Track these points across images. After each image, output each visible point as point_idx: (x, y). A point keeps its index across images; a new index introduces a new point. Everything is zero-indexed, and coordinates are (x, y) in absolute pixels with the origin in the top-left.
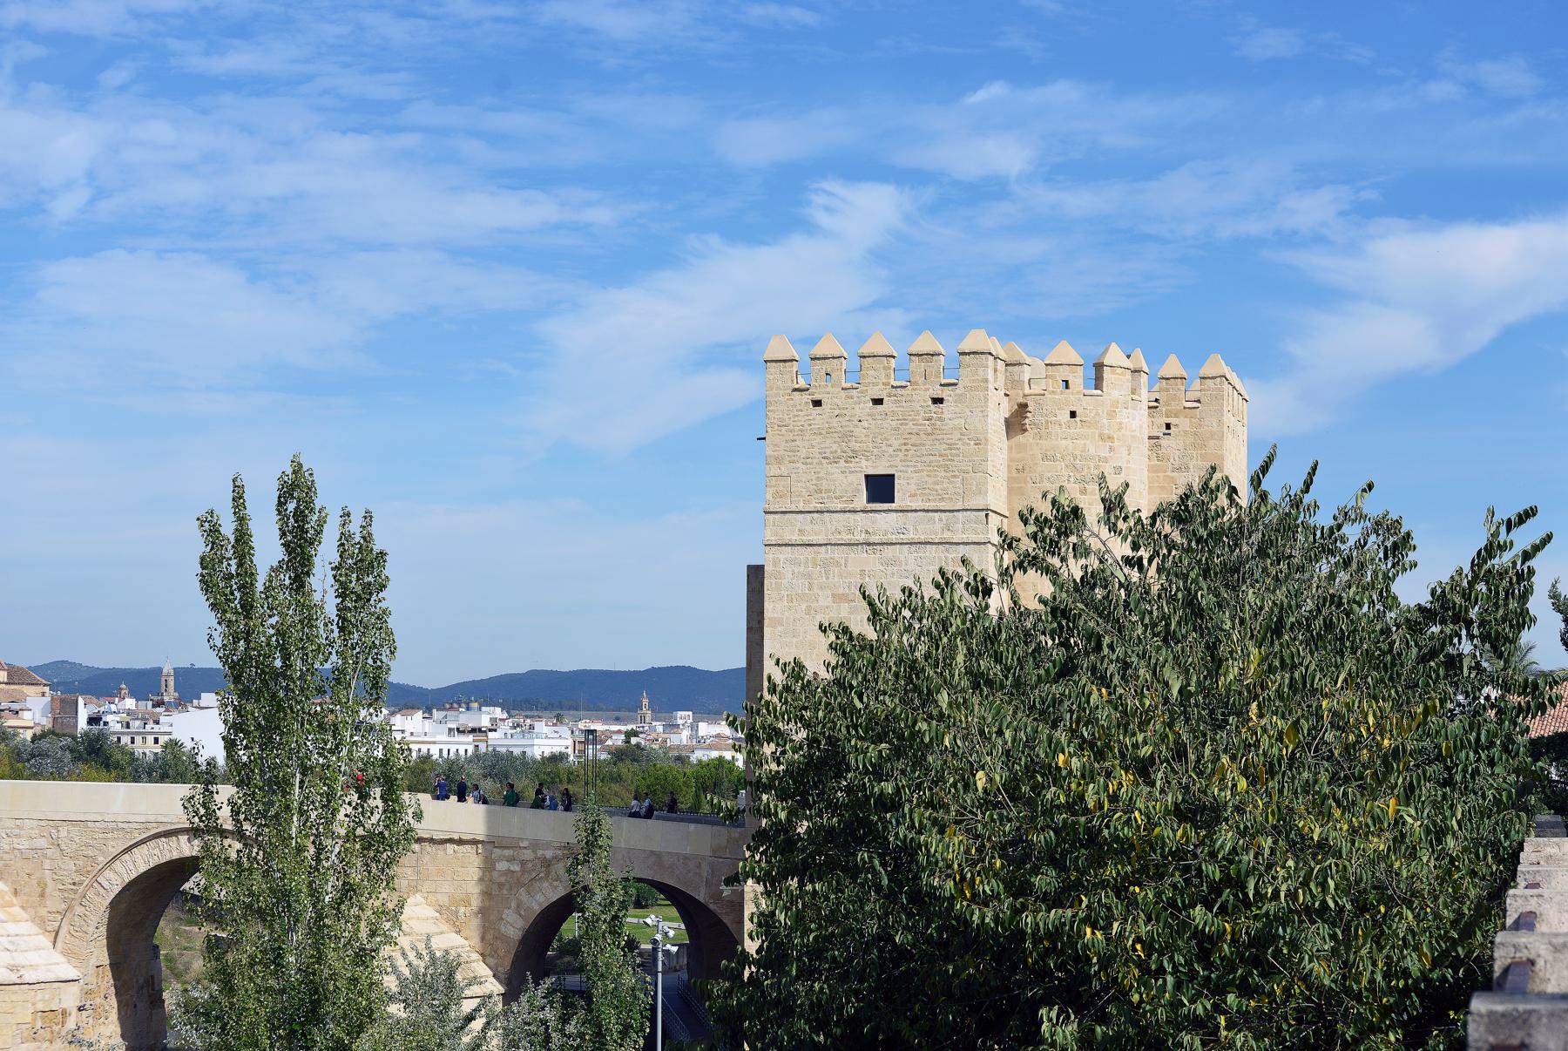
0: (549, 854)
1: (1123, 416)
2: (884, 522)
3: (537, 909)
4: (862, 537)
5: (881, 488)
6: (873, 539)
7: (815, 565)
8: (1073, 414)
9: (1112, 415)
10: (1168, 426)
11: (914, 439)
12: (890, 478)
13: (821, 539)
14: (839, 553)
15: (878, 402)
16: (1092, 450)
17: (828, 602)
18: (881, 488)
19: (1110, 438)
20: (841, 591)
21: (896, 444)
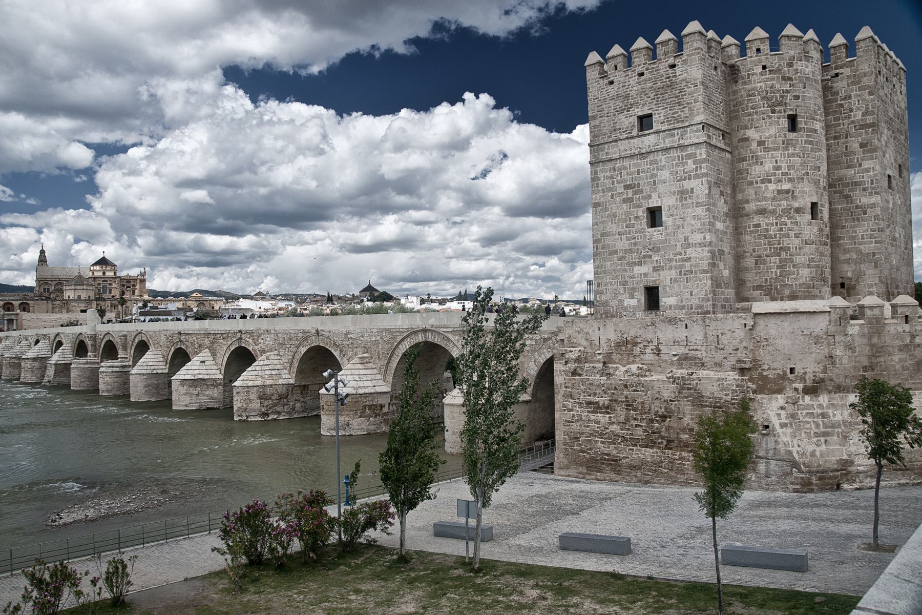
0: (546, 336)
1: (799, 65)
2: (649, 141)
3: (542, 362)
4: (636, 152)
5: (645, 122)
6: (643, 151)
7: (614, 170)
8: (764, 67)
9: (790, 65)
10: (837, 75)
11: (661, 91)
12: (650, 116)
13: (616, 156)
14: (626, 163)
15: (642, 74)
16: (778, 86)
17: (622, 190)
18: (645, 122)
19: (790, 79)
20: (628, 183)
21: (652, 96)
